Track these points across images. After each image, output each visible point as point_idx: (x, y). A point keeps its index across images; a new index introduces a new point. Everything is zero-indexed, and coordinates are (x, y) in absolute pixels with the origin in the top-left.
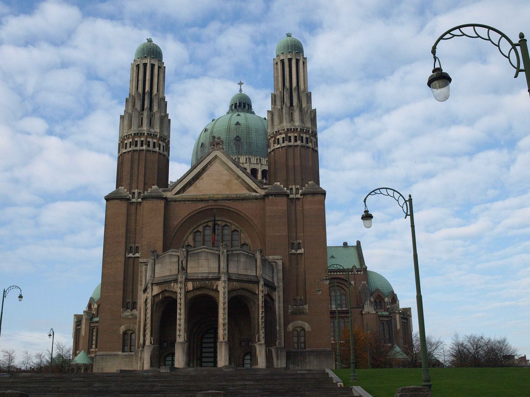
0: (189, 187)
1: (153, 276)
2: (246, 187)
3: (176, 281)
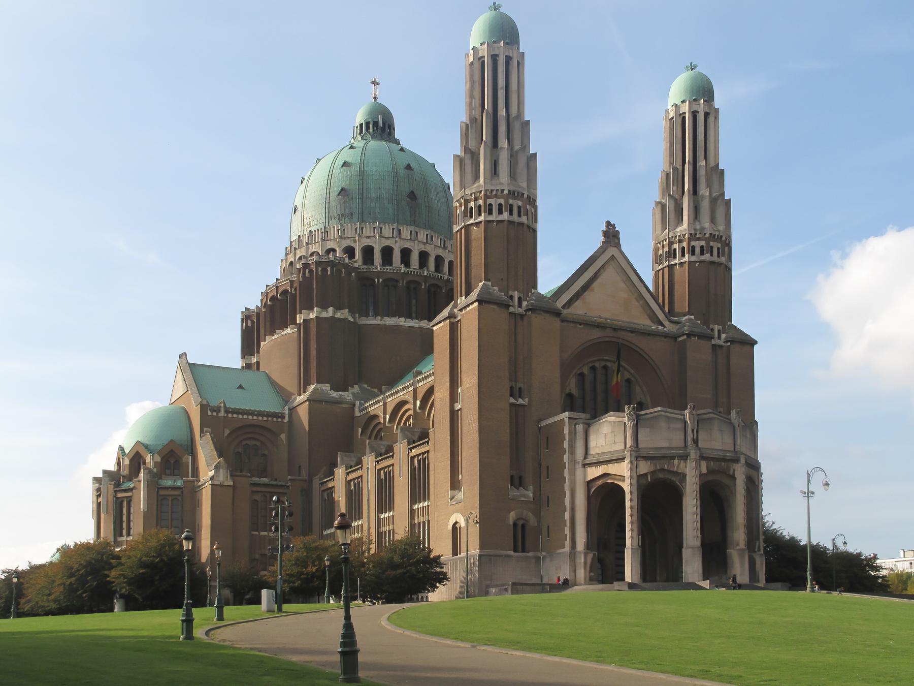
0: (576, 301)
1: (636, 446)
2: (648, 315)
3: (685, 458)
